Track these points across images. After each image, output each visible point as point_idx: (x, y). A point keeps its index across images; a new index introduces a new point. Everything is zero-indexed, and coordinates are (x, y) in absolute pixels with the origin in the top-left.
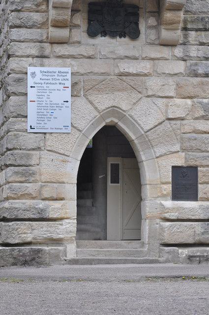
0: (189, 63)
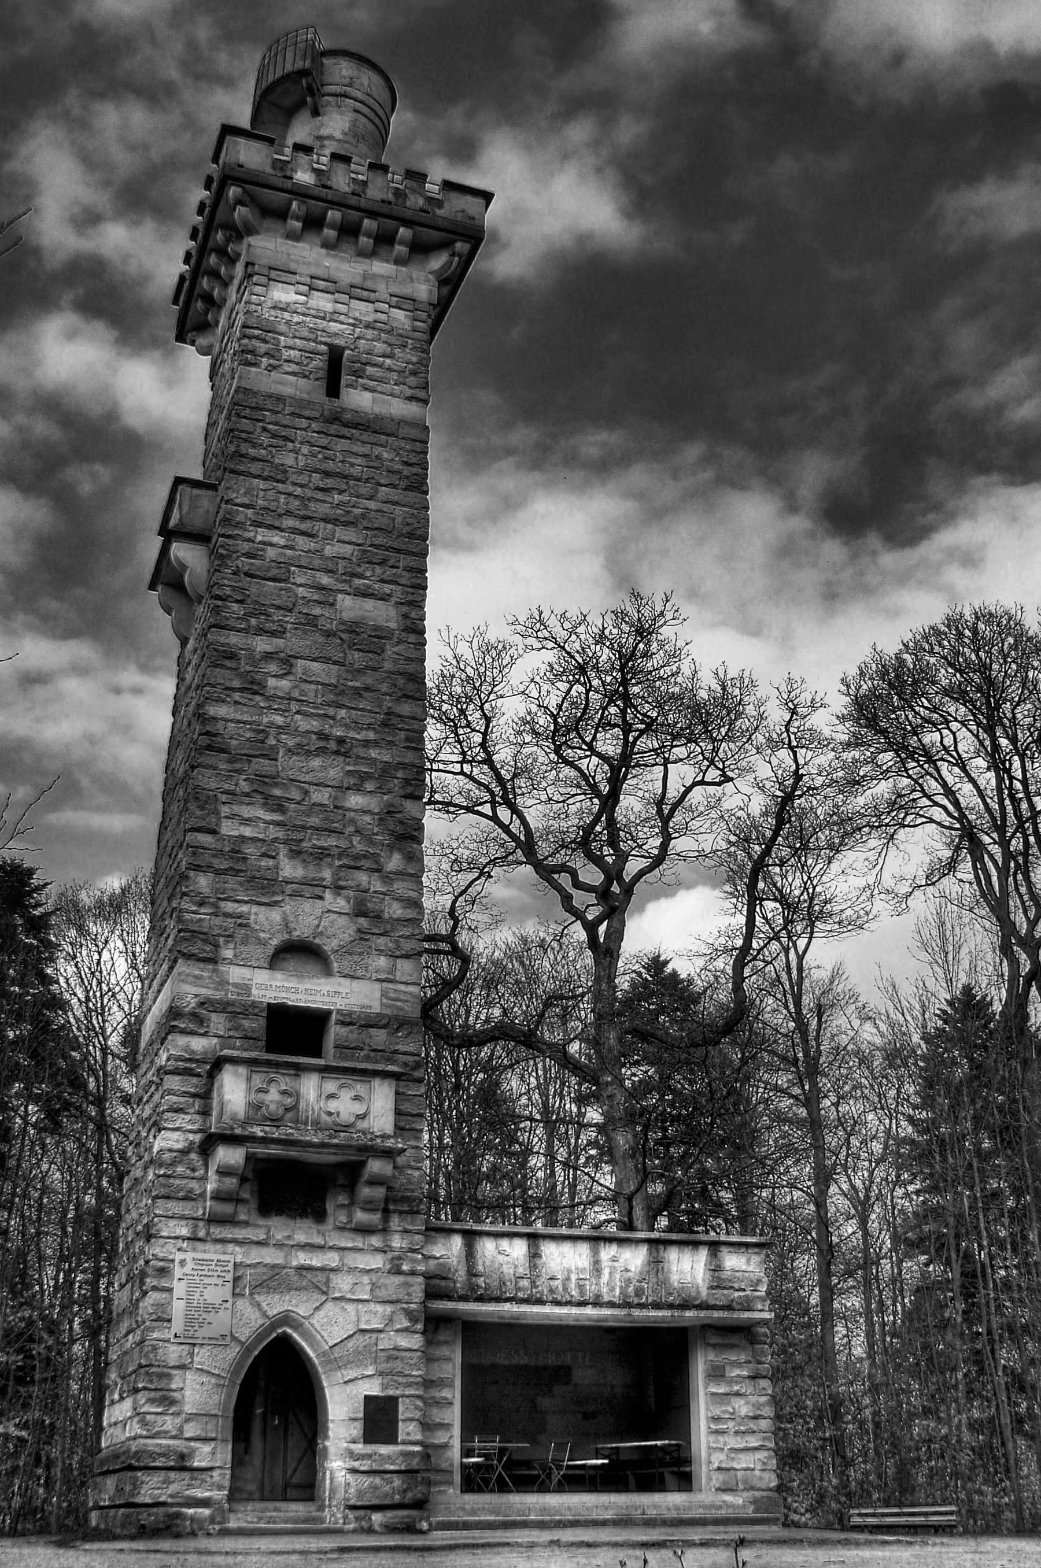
0: (390, 1255)
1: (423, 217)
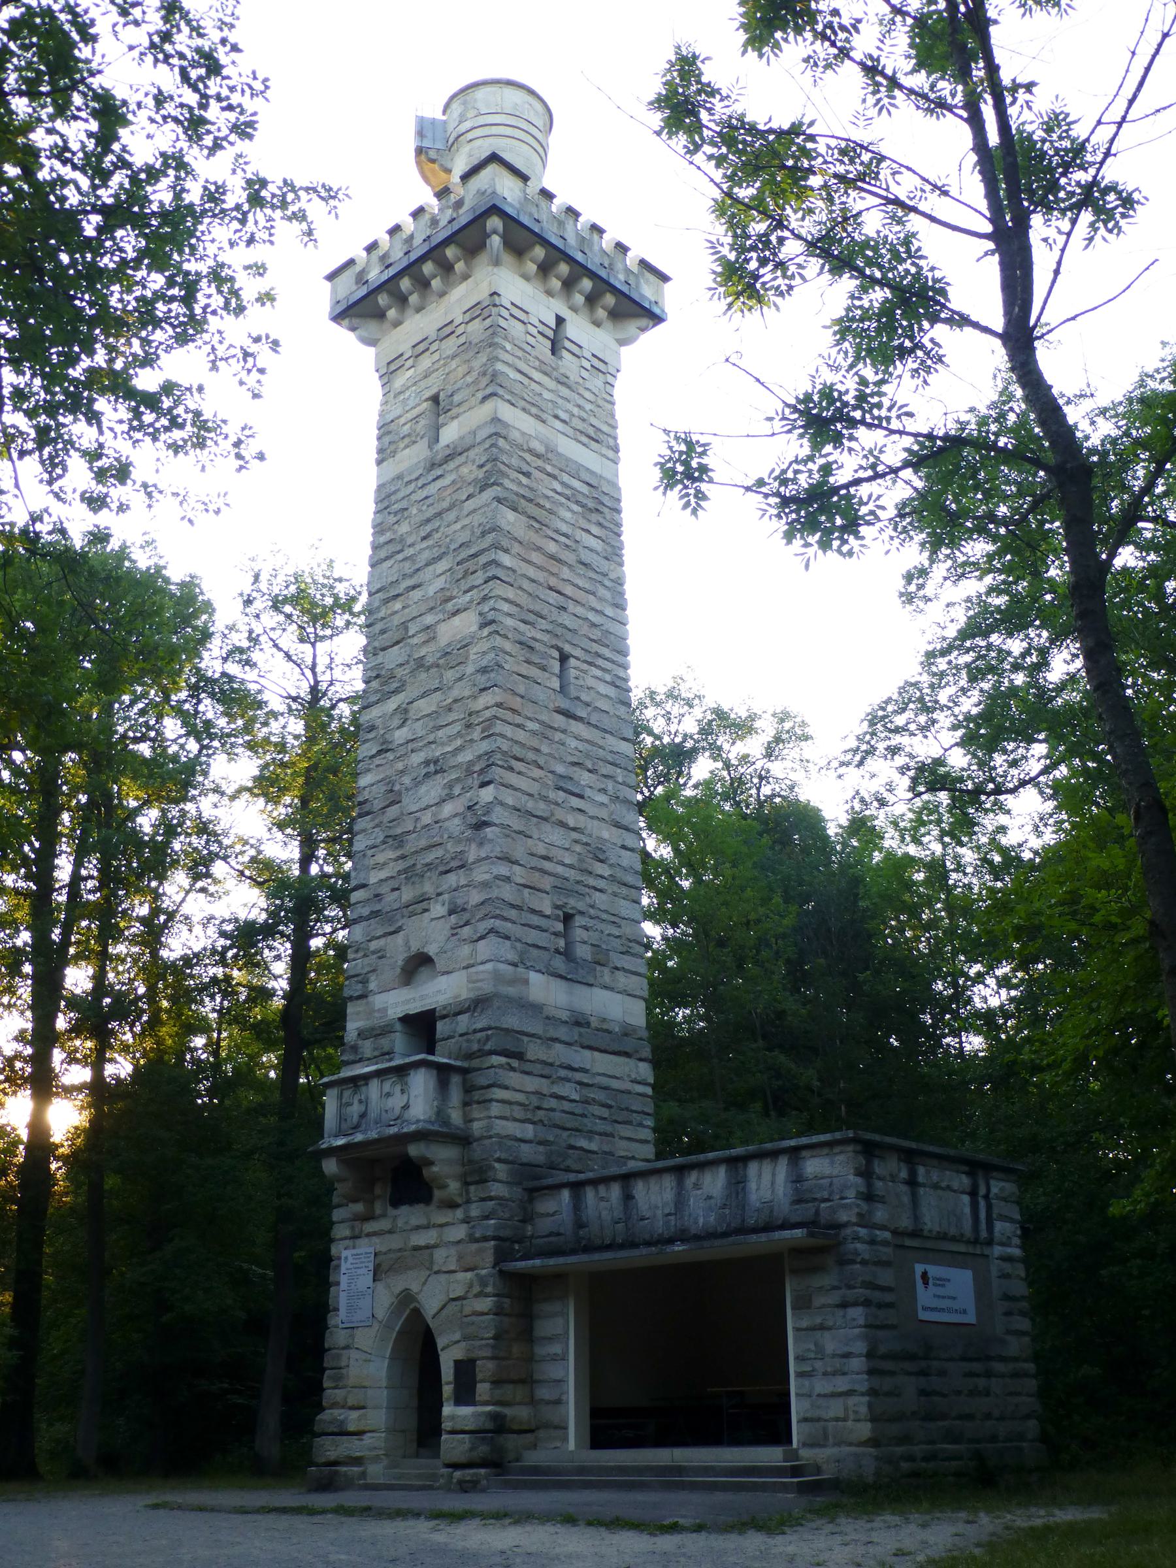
1: (456, 226)
